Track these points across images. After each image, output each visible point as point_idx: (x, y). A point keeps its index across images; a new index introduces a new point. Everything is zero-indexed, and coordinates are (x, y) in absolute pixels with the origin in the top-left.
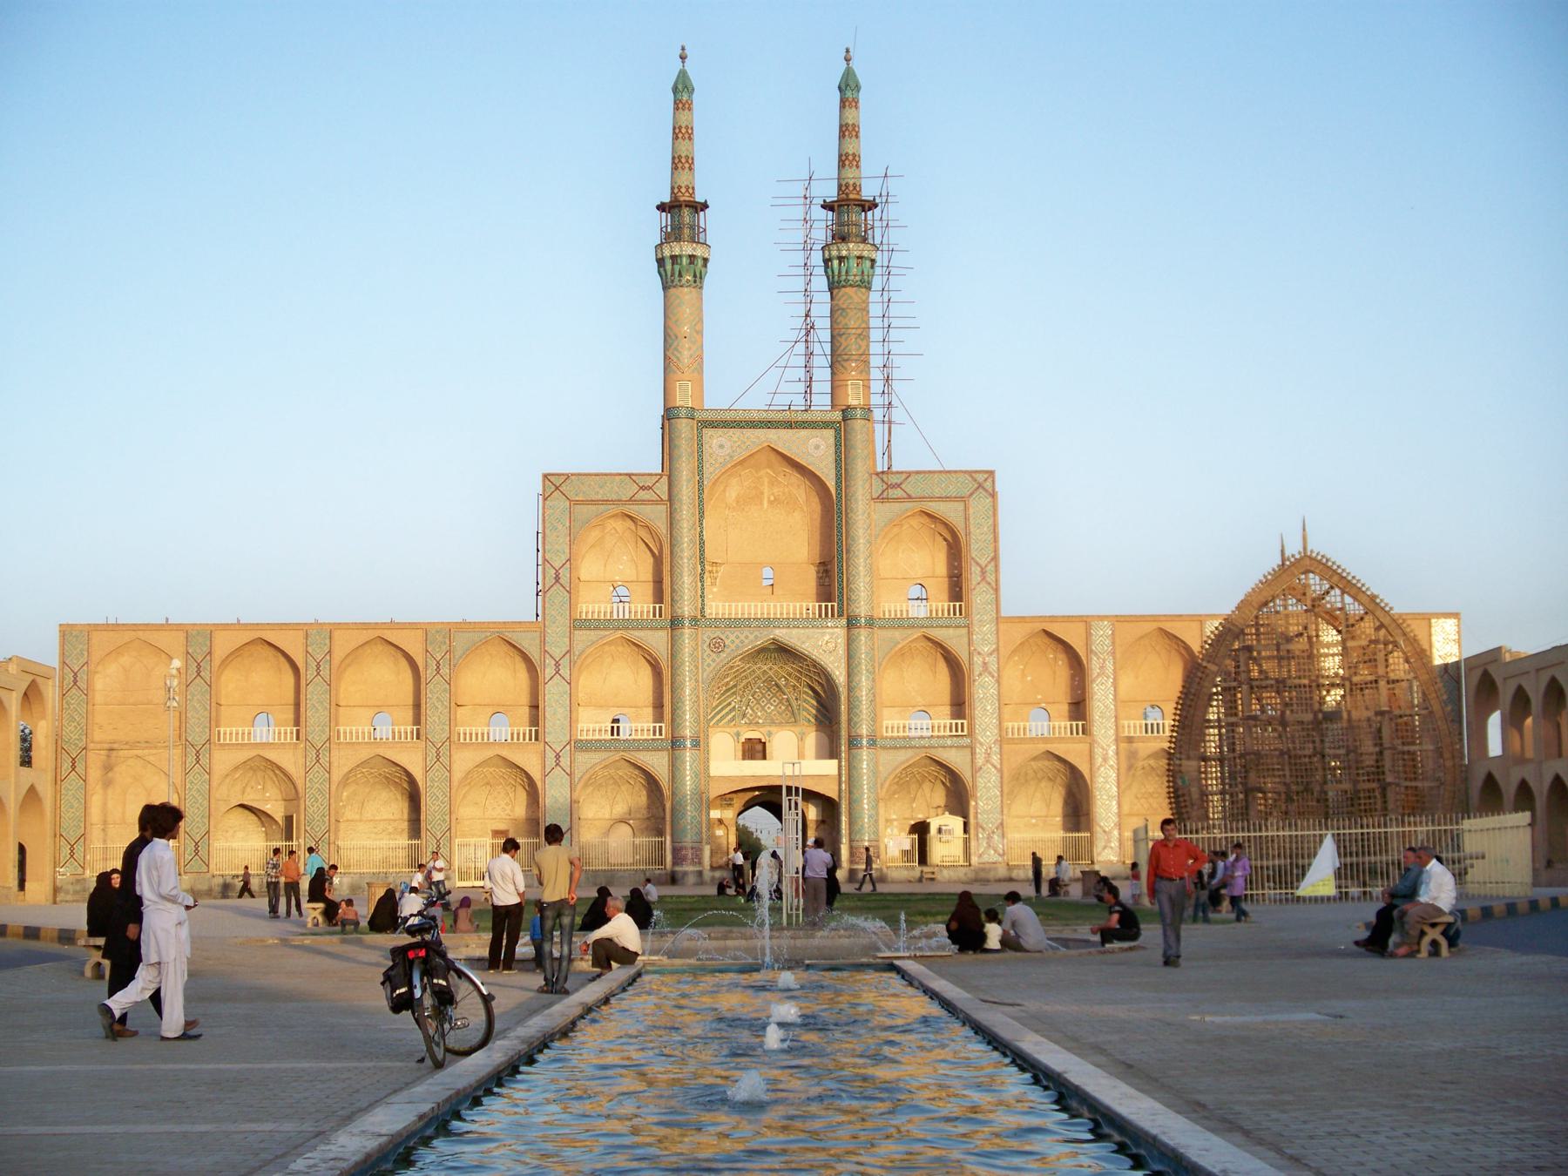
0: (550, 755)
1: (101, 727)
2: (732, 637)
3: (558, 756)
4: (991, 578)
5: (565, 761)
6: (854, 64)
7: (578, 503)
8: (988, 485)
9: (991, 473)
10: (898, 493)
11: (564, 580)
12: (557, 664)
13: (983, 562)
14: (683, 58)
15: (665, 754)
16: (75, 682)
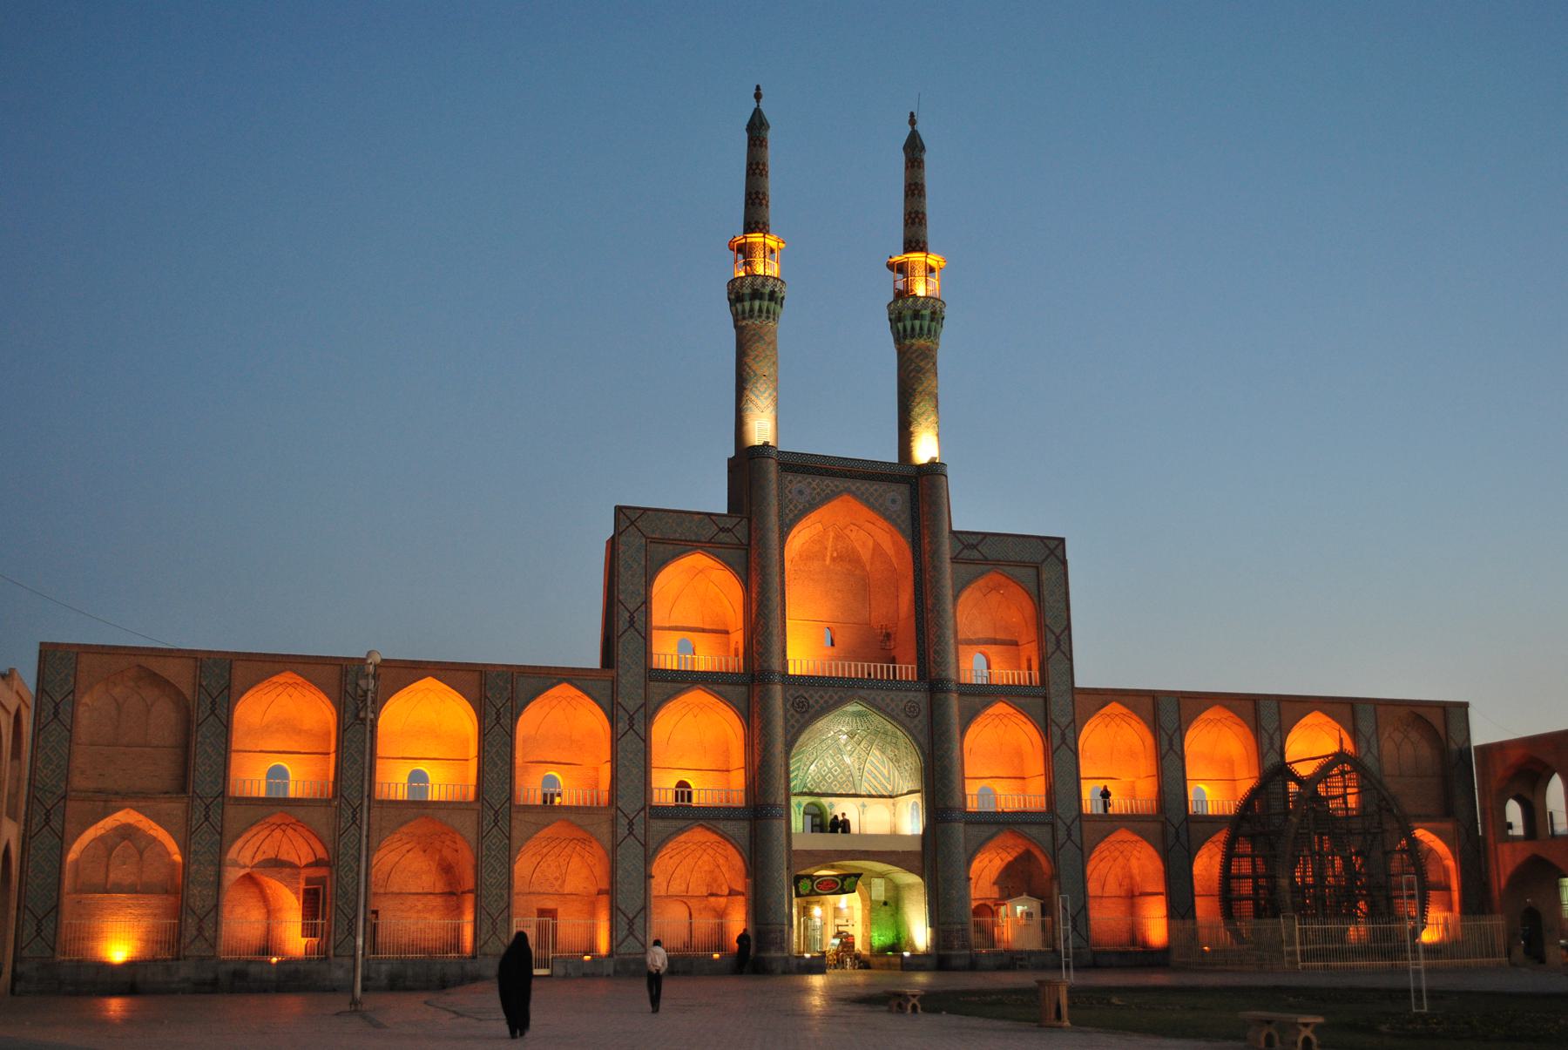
0: (623, 822)
1: (83, 772)
2: (816, 697)
3: (631, 824)
4: (1064, 647)
5: (639, 830)
6: (918, 127)
7: (654, 541)
8: (1058, 552)
9: (1062, 541)
10: (975, 554)
11: (639, 624)
12: (631, 718)
13: (1058, 631)
14: (758, 96)
15: (746, 824)
16: (56, 714)
